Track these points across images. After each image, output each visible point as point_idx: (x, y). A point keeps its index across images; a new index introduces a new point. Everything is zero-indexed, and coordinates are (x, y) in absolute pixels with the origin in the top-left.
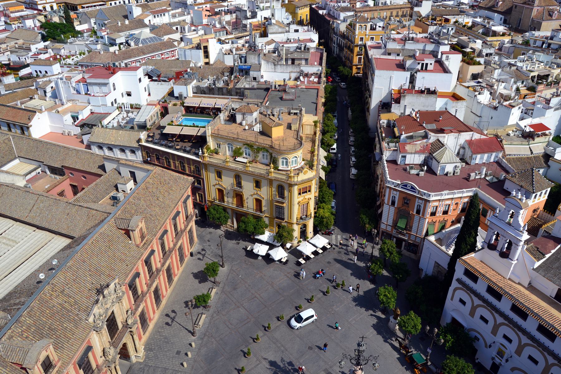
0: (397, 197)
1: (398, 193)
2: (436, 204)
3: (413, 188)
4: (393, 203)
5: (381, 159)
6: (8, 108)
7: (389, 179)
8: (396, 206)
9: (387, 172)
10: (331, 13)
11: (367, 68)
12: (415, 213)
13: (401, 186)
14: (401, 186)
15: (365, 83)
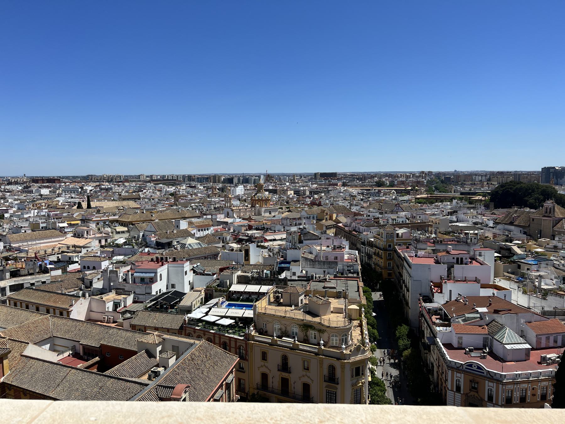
0: (462, 380)
1: (463, 375)
2: (510, 387)
3: (479, 367)
4: (458, 389)
5: (435, 343)
6: (52, 294)
7: (449, 359)
8: (462, 392)
9: (445, 352)
10: (357, 229)
11: (400, 268)
12: (486, 399)
13: (465, 366)
14: (465, 366)
15: (400, 282)
